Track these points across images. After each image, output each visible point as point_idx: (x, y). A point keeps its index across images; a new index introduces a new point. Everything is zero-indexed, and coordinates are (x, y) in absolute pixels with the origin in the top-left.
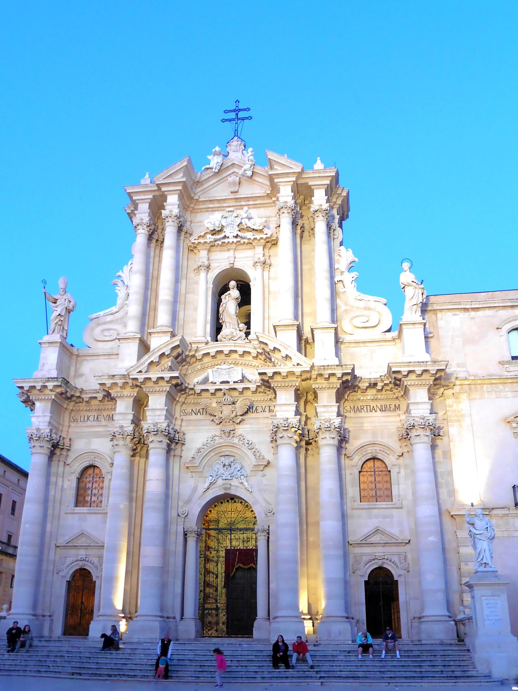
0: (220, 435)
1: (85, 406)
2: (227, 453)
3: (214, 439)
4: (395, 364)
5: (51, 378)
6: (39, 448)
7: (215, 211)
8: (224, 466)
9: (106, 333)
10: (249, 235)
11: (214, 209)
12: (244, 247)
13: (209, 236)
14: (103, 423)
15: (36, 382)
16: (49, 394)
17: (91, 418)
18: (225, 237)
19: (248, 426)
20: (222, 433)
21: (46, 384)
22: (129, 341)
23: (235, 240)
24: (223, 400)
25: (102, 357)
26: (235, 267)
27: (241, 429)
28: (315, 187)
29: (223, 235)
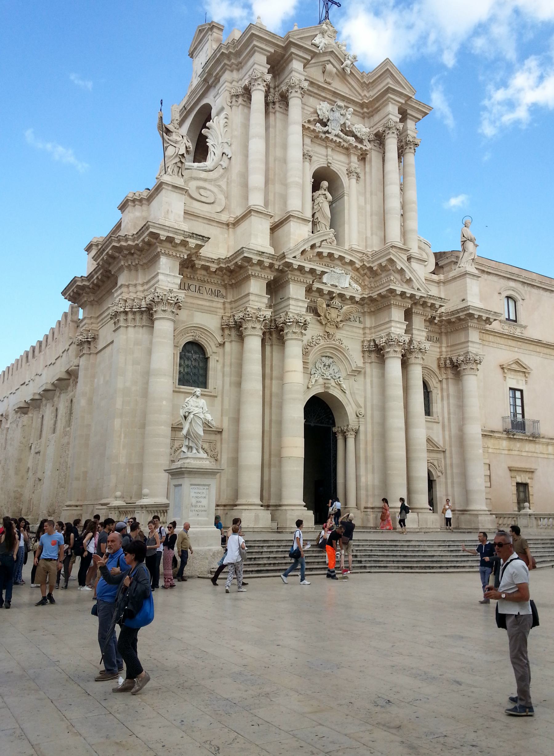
0: (323, 336)
1: (189, 272)
2: (328, 354)
3: (319, 337)
4: (473, 308)
5: (196, 235)
6: (170, 313)
7: (311, 95)
8: (325, 365)
9: (202, 192)
10: (352, 139)
11: (311, 94)
12: (340, 150)
13: (318, 125)
14: (206, 296)
15: (176, 233)
16: (182, 252)
17: (193, 288)
18: (328, 132)
19: (344, 332)
20: (326, 334)
21: (188, 239)
22: (261, 216)
23: (338, 140)
24: (334, 303)
25: (200, 220)
26: (331, 168)
27: (339, 334)
28: (410, 117)
29: (325, 129)
